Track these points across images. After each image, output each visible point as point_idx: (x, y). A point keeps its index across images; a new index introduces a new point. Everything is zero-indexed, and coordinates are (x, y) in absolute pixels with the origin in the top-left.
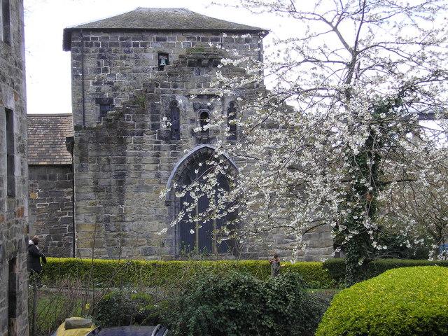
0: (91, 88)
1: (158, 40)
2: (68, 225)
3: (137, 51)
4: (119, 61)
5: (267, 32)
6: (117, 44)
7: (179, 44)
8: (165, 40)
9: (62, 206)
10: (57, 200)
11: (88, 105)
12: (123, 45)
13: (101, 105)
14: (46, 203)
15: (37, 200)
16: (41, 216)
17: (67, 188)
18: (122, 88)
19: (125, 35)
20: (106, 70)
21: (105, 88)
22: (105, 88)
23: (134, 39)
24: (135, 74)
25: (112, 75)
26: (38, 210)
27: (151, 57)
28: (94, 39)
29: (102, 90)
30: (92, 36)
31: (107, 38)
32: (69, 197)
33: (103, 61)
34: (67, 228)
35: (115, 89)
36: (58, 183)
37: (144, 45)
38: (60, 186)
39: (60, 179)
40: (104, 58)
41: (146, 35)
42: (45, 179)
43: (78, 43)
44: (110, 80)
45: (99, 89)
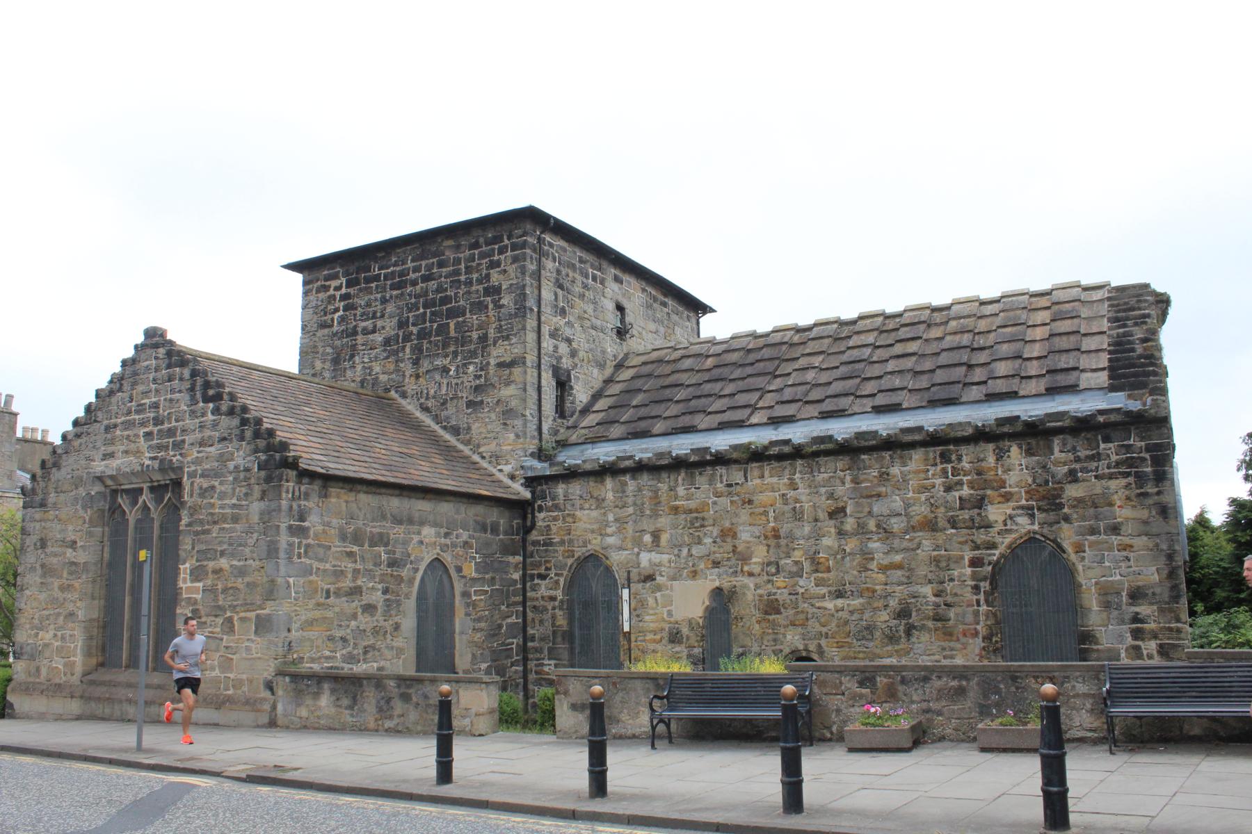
0: (548, 344)
1: (617, 280)
2: (515, 641)
3: (595, 290)
4: (577, 300)
5: (712, 311)
6: (573, 267)
7: (633, 294)
8: (621, 283)
9: (508, 597)
10: (502, 579)
11: (544, 374)
12: (581, 273)
13: (558, 383)
14: (486, 588)
15: (473, 579)
16: (479, 620)
17: (514, 554)
18: (581, 354)
19: (585, 255)
20: (563, 312)
21: (563, 348)
22: (563, 348)
23: (592, 266)
24: (594, 332)
25: (569, 324)
26: (474, 604)
27: (610, 306)
28: (551, 245)
29: (560, 350)
30: (548, 238)
31: (565, 250)
32: (516, 576)
33: (560, 292)
34: (514, 646)
35: (573, 354)
36: (501, 540)
37: (602, 282)
38: (508, 550)
39: (506, 533)
40: (561, 287)
41: (605, 264)
42: (485, 531)
43: (534, 244)
44: (568, 332)
45: (556, 347)
